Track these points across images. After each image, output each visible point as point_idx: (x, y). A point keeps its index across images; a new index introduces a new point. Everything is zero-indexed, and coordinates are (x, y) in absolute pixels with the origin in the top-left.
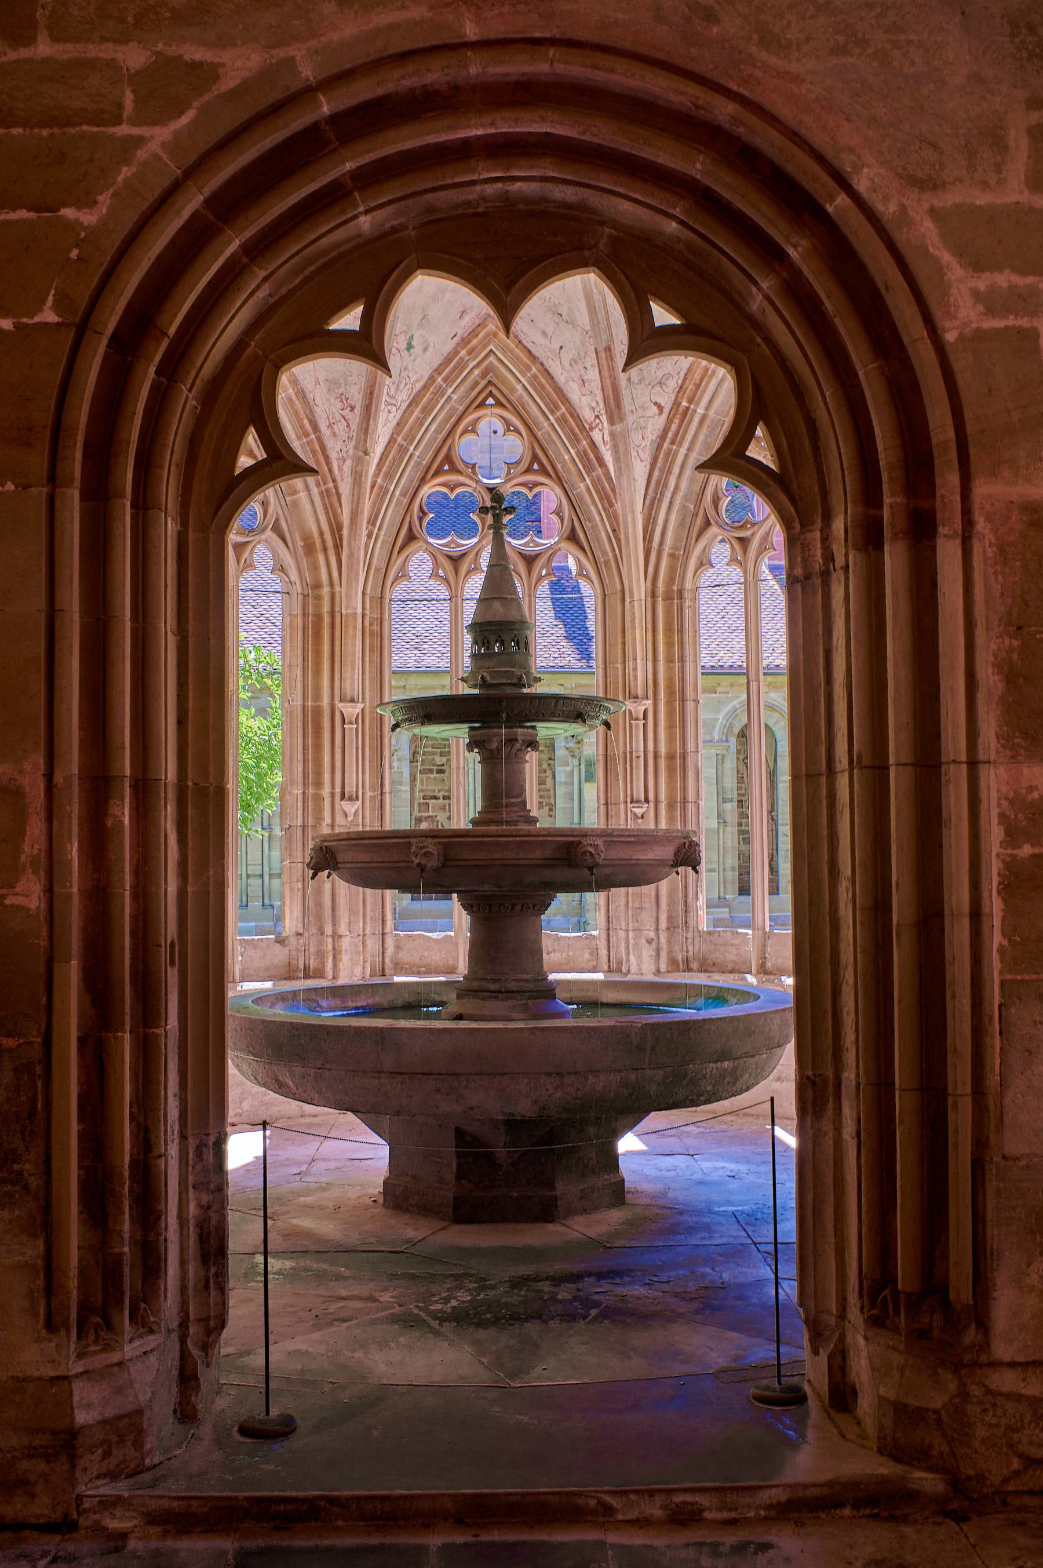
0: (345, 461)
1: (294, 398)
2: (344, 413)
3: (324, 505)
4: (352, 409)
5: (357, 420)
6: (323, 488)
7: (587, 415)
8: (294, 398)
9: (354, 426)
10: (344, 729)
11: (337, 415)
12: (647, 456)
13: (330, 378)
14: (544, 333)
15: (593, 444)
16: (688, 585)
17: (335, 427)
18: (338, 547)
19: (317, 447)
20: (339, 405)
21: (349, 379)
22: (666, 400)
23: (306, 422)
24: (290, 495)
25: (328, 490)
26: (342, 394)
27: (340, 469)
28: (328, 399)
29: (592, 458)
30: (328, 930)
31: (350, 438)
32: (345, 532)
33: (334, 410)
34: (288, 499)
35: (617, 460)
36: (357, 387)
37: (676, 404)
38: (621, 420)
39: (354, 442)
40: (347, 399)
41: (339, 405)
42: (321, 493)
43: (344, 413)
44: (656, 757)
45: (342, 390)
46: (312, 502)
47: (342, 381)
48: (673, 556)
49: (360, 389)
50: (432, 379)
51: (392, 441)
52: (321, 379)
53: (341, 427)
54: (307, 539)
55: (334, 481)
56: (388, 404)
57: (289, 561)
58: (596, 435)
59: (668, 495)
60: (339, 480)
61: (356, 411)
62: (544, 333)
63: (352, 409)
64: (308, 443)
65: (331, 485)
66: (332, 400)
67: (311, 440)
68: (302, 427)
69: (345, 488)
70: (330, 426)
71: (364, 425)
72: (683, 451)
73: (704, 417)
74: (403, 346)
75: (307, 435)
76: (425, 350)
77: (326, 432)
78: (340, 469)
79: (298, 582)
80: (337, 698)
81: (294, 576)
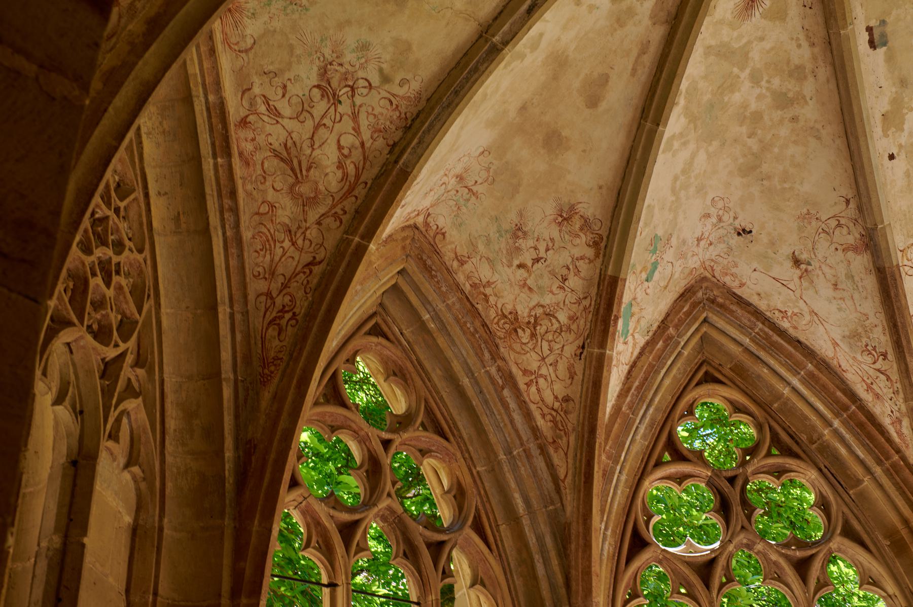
0: (900, 421)
1: (816, 372)
2: (878, 366)
3: (896, 484)
4: (885, 356)
5: (895, 366)
6: (887, 464)
8: (816, 372)
9: (895, 377)
11: (872, 372)
13: (847, 333)
17: (874, 386)
19: (863, 419)
21: (867, 323)
23: (839, 394)
24: (852, 487)
25: (894, 466)
26: (867, 345)
27: (900, 434)
28: (854, 358)
31: (896, 392)
33: (866, 368)
34: (851, 492)
36: (880, 329)
39: (901, 395)
40: (874, 348)
41: (869, 360)
42: (887, 472)
43: (878, 366)
45: (864, 340)
46: (881, 486)
47: (860, 330)
49: (884, 329)
52: (837, 335)
54: (891, 534)
55: (898, 451)
57: (876, 569)
60: (904, 448)
64: (850, 417)
65: (896, 457)
66: (859, 357)
67: (854, 412)
68: (837, 401)
70: (869, 388)
71: (903, 366)
75: (846, 408)
78: (900, 434)
79: (897, 593)
81: (891, 588)
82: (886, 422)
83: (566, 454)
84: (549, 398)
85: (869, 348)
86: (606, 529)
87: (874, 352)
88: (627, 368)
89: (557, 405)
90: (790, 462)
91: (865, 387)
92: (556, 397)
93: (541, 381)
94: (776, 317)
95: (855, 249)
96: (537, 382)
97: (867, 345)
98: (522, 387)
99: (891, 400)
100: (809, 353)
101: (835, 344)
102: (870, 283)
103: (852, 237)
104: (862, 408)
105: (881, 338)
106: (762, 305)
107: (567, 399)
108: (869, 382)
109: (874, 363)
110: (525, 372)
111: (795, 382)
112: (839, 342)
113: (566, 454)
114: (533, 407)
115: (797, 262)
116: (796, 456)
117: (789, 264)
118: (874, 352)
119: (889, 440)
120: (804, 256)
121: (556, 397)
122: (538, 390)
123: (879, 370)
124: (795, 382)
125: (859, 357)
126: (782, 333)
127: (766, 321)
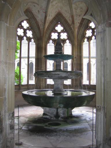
7: (70, 24)
9: (43, 25)
12: (77, 29)
14: (65, 14)
15: (71, 27)
16: (82, 44)
18: (41, 39)
22: (80, 22)
29: (71, 29)
32: (42, 37)
35: (74, 29)
37: (81, 22)
38: (74, 24)
44: (78, 64)
48: (80, 41)
50: (52, 20)
51: (48, 27)
53: (42, 25)
58: (71, 26)
59: (80, 33)
62: (65, 14)
69: (42, 32)
72: (81, 28)
73: (84, 24)
74: (49, 15)
76: (51, 16)
77: (40, 26)
82: (41, 28)
94: (34, 15)
95: (44, 13)
102: (44, 16)
103: (44, 11)
105: (43, 21)
106: (34, 14)
111: (34, 22)
115: (38, 11)
117: (38, 11)
120: (39, 11)
126: (34, 17)
127: (33, 15)
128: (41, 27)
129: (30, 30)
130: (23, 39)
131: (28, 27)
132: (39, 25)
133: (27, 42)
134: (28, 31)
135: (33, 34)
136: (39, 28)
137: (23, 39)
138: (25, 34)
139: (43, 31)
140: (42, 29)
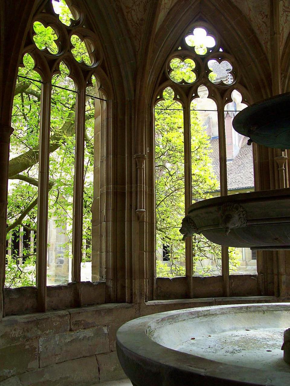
0: (267, 42)
2: (263, 20)
4: (267, 16)
10: (278, 170)
17: (261, 28)
20: (261, 17)
30: (275, 272)
40: (264, 13)
41: (261, 17)
55: (264, 54)
56: (285, 11)
61: (268, 16)
63: (267, 16)
66: (258, 16)
77: (257, 32)
78: (266, 47)
80: (275, 156)
82: (262, 42)
83: (140, 41)
84: (135, 18)
85: (262, 13)
86: (152, 72)
87: (263, 14)
88: (168, 10)
89: (138, 22)
90: (227, 55)
91: (258, 28)
92: (138, 19)
93: (133, 11)
96: (131, 12)
97: (261, 11)
98: (125, 14)
99: (266, 34)
100: (240, 12)
101: (250, 10)
104: (255, 36)
105: (266, 9)
107: (142, 20)
108: (259, 26)
109: (263, 19)
110: (127, 7)
111: (233, 23)
112: (252, 9)
113: (140, 41)
114: (128, 22)
116: (228, 53)
118: (263, 14)
119: (262, 49)
121: (138, 19)
122: (131, 16)
123: (263, 22)
124: (233, 23)
125: (258, 16)
128: (264, 38)
129: (220, 58)
130: (197, 96)
131: (213, 49)
132: (253, 31)
133: (212, 105)
134: (212, 64)
135: (234, 73)
136: (255, 42)
137: (197, 96)
138: (203, 73)
139: (274, 48)
140: (269, 44)
